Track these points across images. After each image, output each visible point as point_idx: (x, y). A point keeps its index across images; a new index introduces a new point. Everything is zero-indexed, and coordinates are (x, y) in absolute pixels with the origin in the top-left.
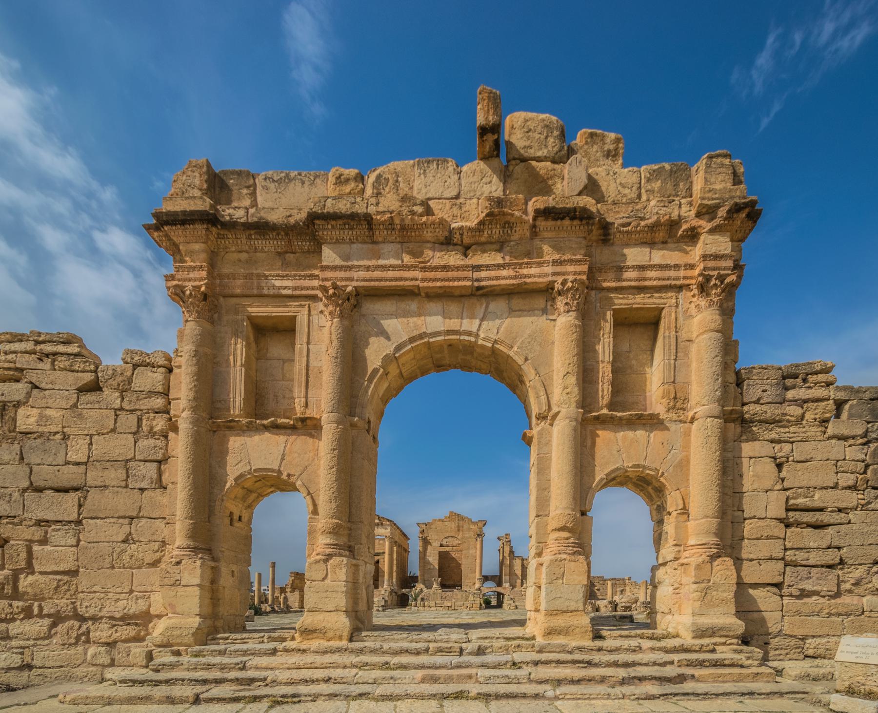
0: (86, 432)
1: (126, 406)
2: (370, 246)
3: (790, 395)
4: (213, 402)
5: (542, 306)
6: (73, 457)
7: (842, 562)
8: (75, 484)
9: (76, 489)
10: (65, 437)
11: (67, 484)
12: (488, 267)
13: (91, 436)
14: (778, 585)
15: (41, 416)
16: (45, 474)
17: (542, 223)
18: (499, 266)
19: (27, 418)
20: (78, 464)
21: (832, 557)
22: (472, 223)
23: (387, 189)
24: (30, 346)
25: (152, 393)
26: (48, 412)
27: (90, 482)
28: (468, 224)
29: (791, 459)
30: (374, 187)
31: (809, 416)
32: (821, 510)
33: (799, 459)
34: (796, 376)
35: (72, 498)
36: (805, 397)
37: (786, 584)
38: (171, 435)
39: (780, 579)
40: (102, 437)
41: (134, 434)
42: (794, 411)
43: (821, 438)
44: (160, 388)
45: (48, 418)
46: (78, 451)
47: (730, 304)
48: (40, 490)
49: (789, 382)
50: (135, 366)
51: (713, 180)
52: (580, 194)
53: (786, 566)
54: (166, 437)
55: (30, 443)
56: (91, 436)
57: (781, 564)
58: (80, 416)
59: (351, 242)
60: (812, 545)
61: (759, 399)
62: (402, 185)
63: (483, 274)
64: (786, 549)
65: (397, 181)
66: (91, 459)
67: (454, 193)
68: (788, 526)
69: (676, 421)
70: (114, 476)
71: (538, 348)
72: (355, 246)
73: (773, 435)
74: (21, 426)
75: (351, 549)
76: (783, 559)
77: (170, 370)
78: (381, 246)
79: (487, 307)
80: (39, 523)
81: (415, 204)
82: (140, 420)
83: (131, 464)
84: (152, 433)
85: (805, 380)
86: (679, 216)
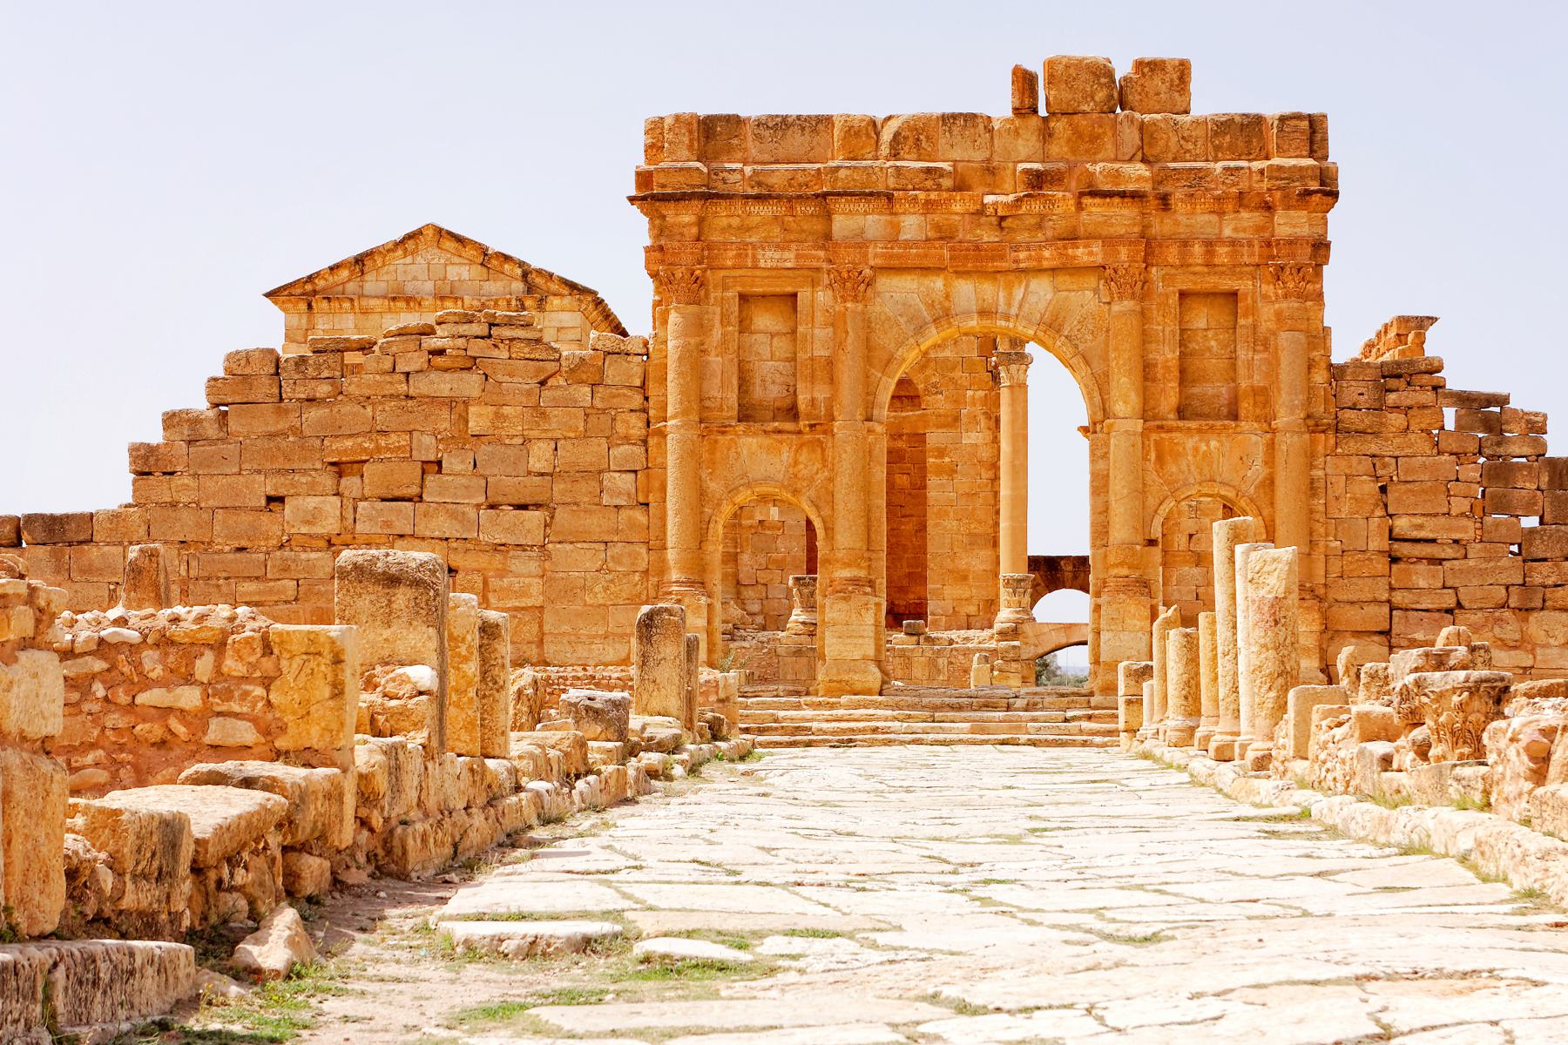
0: (550, 435)
1: (598, 403)
2: (889, 218)
3: (1392, 398)
4: (701, 400)
5: (1094, 285)
6: (537, 465)
7: (1459, 605)
8: (539, 499)
9: (538, 506)
10: (526, 441)
11: (528, 500)
13: (556, 440)
14: (1387, 633)
15: (497, 415)
16: (510, 485)
17: (1087, 200)
20: (542, 474)
21: (1450, 601)
22: (1011, 198)
23: (907, 148)
26: (506, 410)
27: (557, 497)
29: (1395, 478)
30: (891, 147)
32: (1433, 541)
33: (1402, 478)
34: (1399, 376)
35: (534, 516)
36: (1409, 402)
37: (1394, 632)
38: (652, 441)
39: (1386, 626)
40: (569, 442)
41: (607, 438)
42: (1396, 420)
43: (1429, 452)
45: (506, 418)
46: (540, 458)
47: (1318, 286)
48: (492, 507)
49: (1393, 383)
51: (1285, 147)
52: (1130, 160)
53: (1391, 610)
54: (645, 442)
55: (484, 450)
56: (556, 440)
57: (1386, 609)
59: (866, 213)
60: (1422, 584)
61: (1355, 404)
62: (924, 144)
63: (1022, 255)
64: (1392, 589)
65: (918, 139)
66: (558, 470)
67: (987, 154)
68: (1395, 560)
70: (584, 490)
71: (1090, 337)
72: (870, 217)
73: (1373, 448)
74: (474, 426)
76: (1389, 601)
78: (902, 218)
79: (1027, 286)
81: (942, 176)
82: (614, 420)
83: (606, 475)
84: (627, 439)
86: (1250, 186)
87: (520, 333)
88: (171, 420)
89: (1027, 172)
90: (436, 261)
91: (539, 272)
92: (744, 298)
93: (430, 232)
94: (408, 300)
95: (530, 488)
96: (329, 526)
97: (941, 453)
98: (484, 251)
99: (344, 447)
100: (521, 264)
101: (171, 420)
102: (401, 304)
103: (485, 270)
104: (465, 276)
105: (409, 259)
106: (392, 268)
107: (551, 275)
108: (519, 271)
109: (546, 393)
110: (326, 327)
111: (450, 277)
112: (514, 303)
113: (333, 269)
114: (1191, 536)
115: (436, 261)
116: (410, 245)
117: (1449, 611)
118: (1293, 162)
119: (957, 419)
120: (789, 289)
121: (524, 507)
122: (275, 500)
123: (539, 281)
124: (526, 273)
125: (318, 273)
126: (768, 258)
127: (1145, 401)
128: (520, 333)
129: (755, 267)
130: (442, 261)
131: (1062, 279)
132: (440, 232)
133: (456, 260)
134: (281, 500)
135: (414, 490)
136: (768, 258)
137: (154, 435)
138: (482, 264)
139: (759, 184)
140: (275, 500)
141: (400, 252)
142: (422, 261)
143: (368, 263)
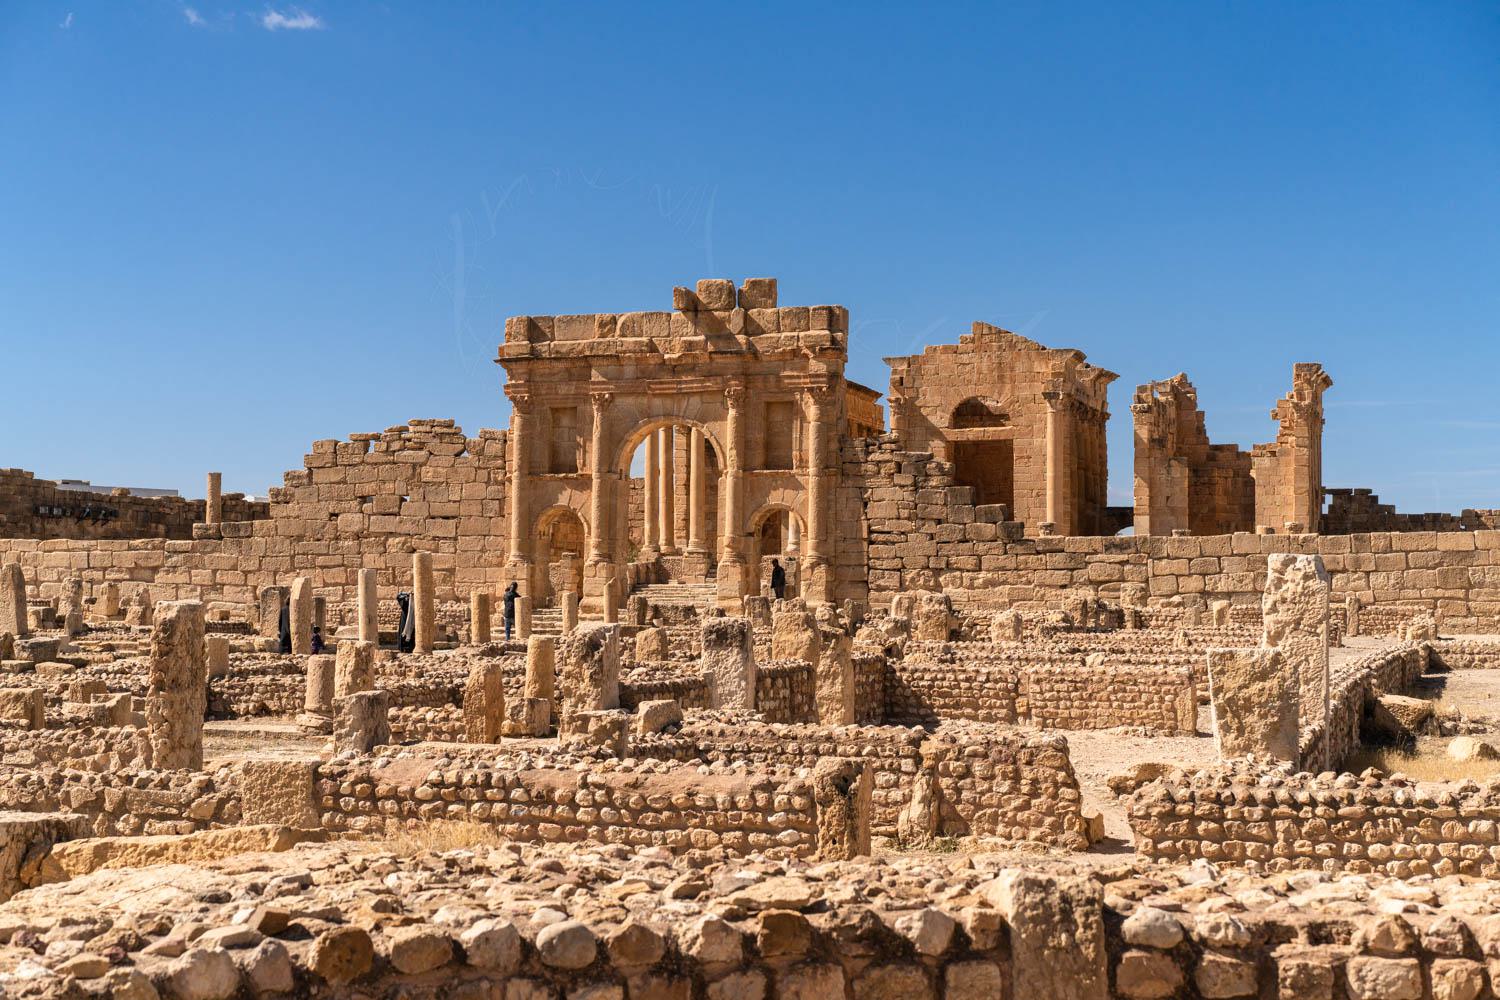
9: (453, 517)
11: (449, 515)
12: (686, 382)
16: (437, 509)
18: (692, 382)
19: (427, 473)
20: (455, 502)
24: (428, 429)
25: (496, 457)
28: (674, 356)
31: (882, 471)
44: (500, 454)
48: (433, 518)
50: (486, 440)
58: (456, 472)
75: (610, 557)
77: (505, 441)
80: (434, 538)
82: (489, 474)
85: (880, 448)
87: (445, 430)
88: (288, 476)
89: (685, 342)
92: (555, 411)
95: (451, 509)
96: (356, 528)
97: (1021, 450)
99: (368, 489)
101: (288, 476)
109: (458, 460)
114: (1168, 498)
117: (899, 570)
118: (818, 332)
119: (1032, 430)
120: (573, 405)
121: (447, 518)
122: (334, 515)
126: (563, 389)
127: (745, 460)
128: (445, 430)
129: (557, 394)
131: (707, 398)
134: (337, 515)
135: (396, 510)
136: (563, 389)
137: (281, 484)
139: (557, 352)
140: (334, 515)
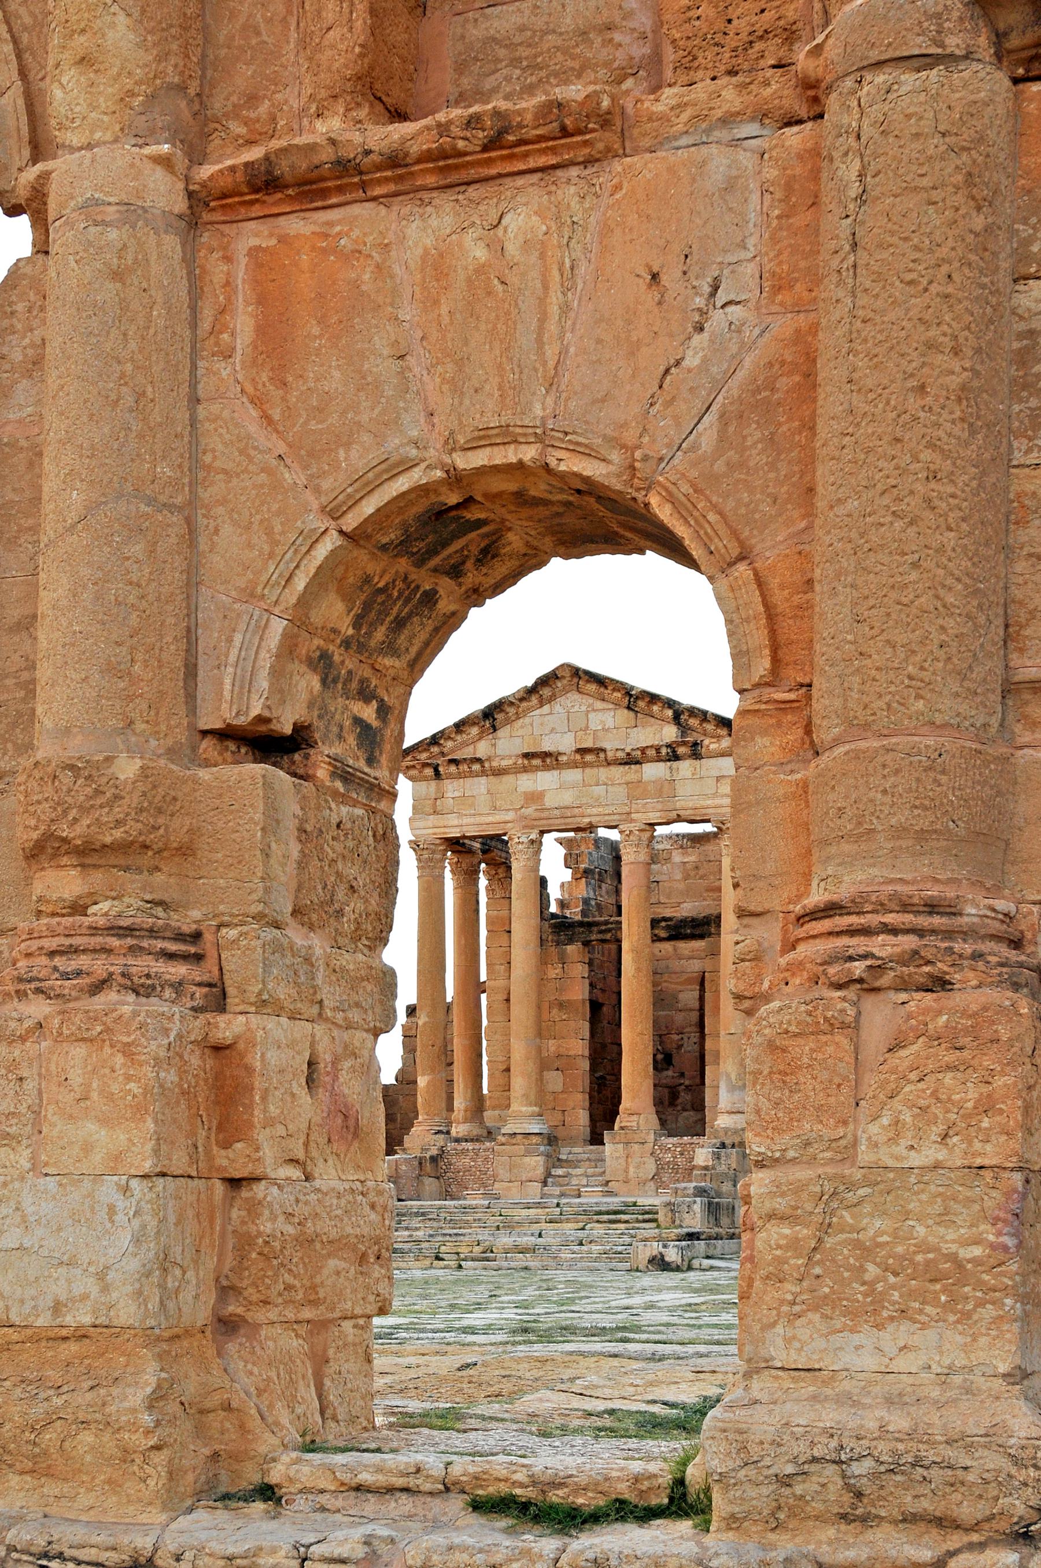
69: (727, 120)
90: (576, 708)
91: (693, 711)
93: (567, 674)
94: (546, 755)
98: (627, 691)
100: (670, 703)
102: (536, 762)
103: (632, 714)
104: (610, 723)
105: (546, 709)
106: (527, 720)
107: (705, 713)
108: (670, 713)
110: (457, 794)
111: (593, 726)
112: (664, 751)
113: (460, 726)
115: (576, 708)
116: (546, 692)
123: (693, 722)
124: (679, 714)
125: (442, 732)
130: (584, 708)
132: (576, 672)
133: (599, 705)
138: (629, 708)
141: (534, 700)
142: (561, 710)
143: (500, 717)
